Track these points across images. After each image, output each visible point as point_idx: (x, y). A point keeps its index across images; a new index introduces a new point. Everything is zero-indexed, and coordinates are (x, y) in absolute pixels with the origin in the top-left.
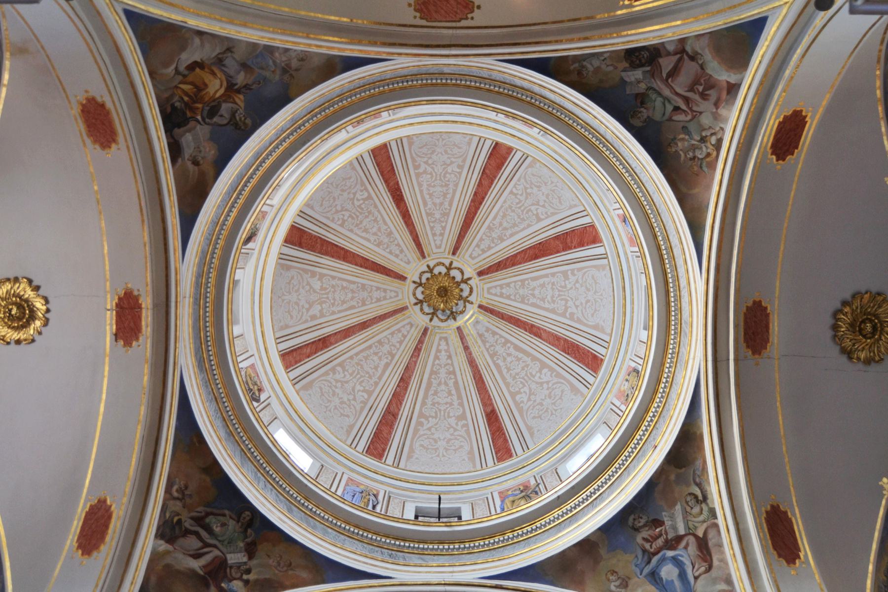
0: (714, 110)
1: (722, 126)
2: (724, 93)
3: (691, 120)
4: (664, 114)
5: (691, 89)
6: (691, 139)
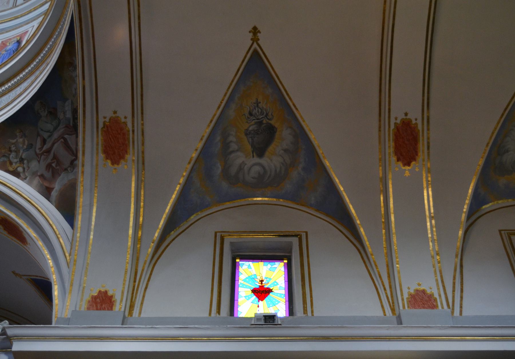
0: (39, 174)
1: (28, 178)
2: (47, 184)
3: (36, 152)
4: (42, 130)
5: (55, 157)
6: (24, 150)
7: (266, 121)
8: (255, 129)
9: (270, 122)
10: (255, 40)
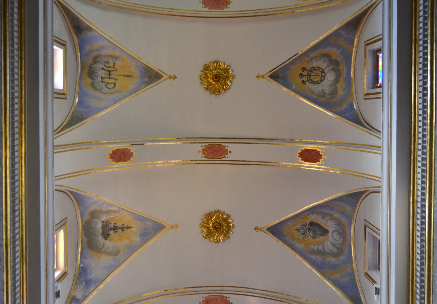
7: (307, 226)
8: (312, 232)
9: (308, 224)
10: (261, 230)
